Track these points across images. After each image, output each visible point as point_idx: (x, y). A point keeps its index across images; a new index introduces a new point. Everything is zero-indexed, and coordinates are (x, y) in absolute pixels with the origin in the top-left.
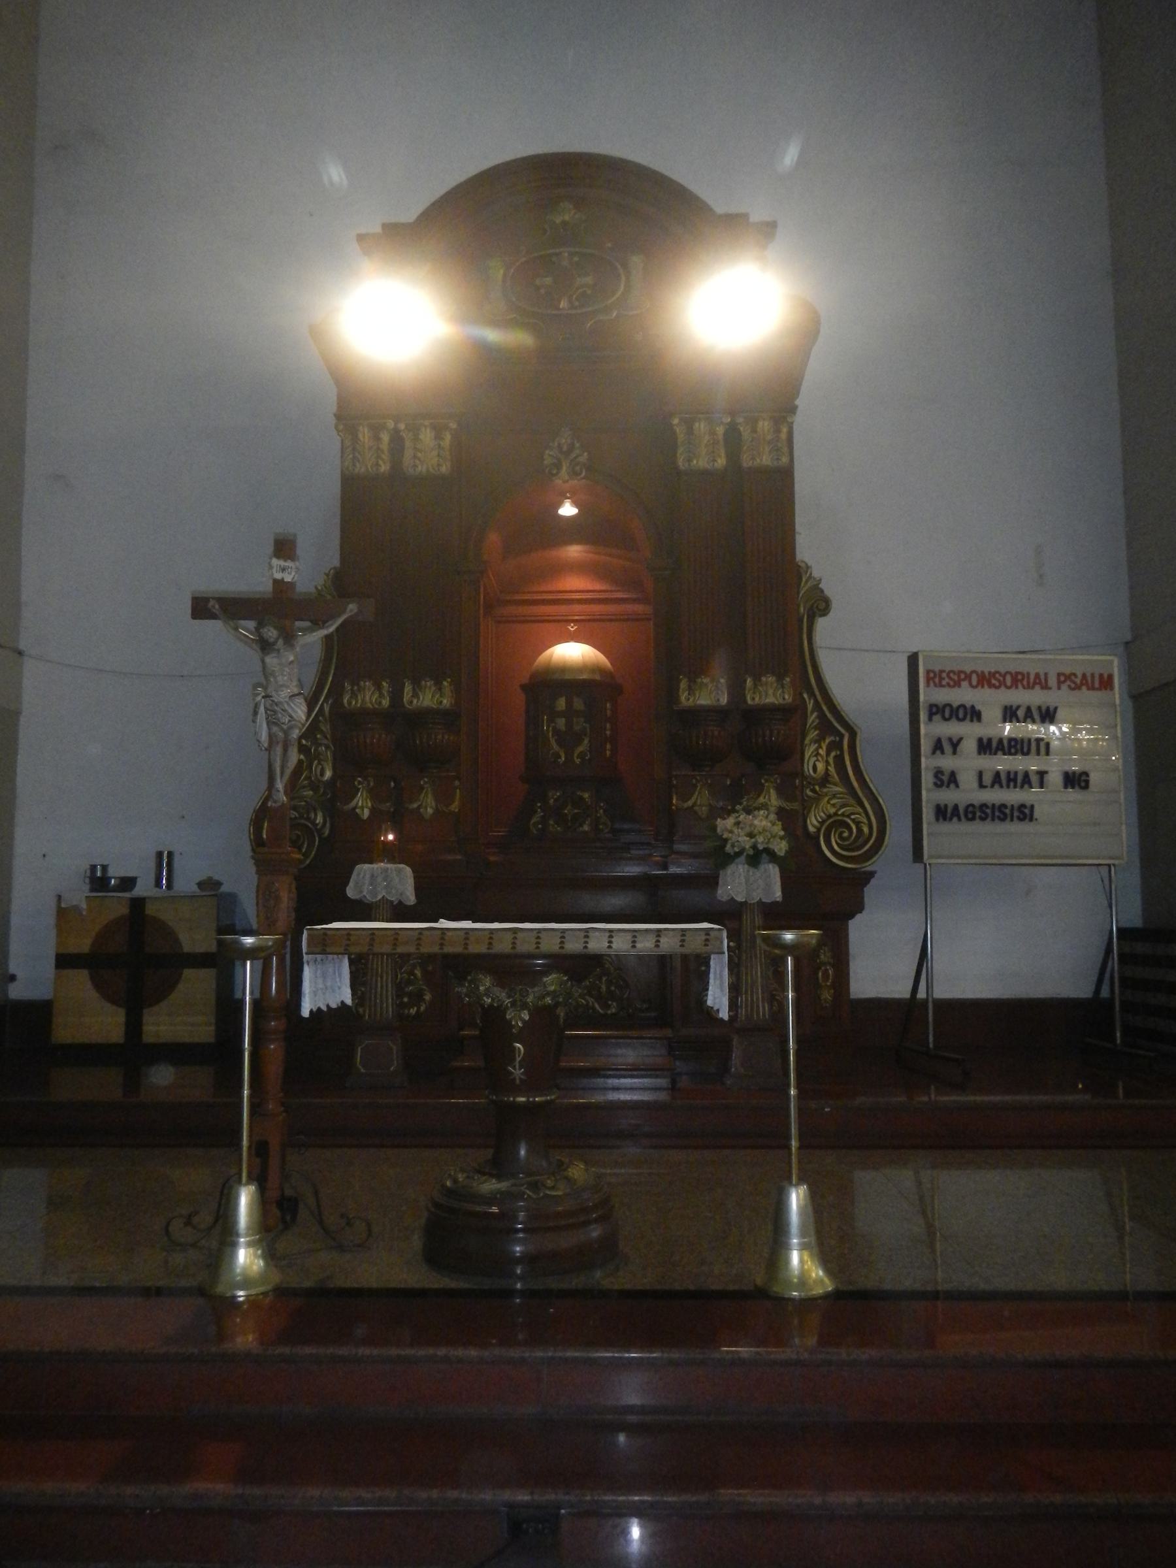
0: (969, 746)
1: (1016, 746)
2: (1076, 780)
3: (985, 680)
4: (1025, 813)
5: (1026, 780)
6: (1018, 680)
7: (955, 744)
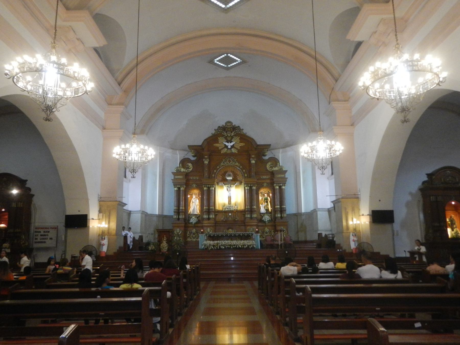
0: (39, 235)
1: (44, 235)
2: (51, 239)
3: (42, 228)
4: (45, 242)
5: (45, 239)
6: (46, 228)
7: (38, 235)
